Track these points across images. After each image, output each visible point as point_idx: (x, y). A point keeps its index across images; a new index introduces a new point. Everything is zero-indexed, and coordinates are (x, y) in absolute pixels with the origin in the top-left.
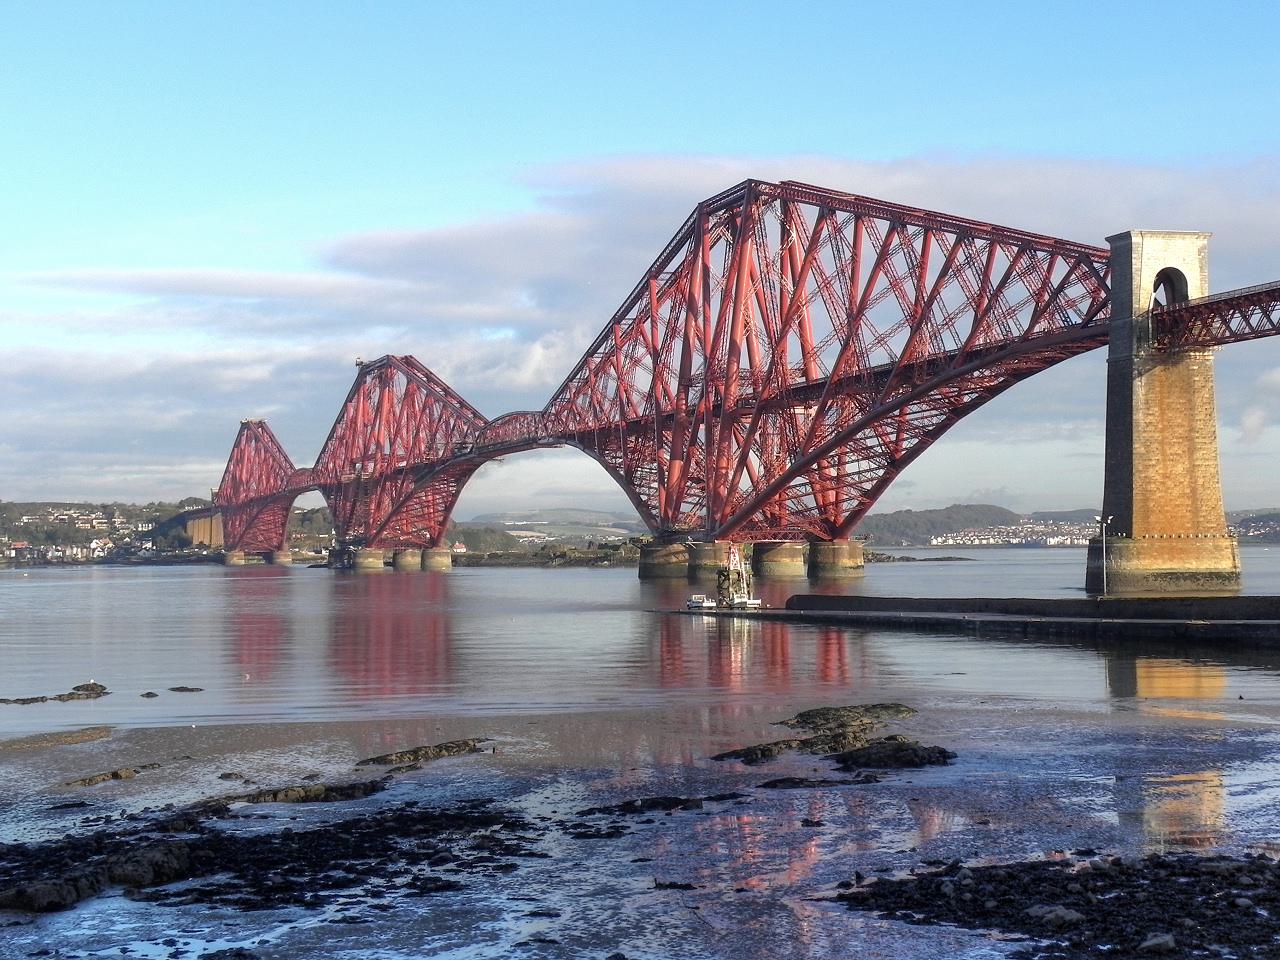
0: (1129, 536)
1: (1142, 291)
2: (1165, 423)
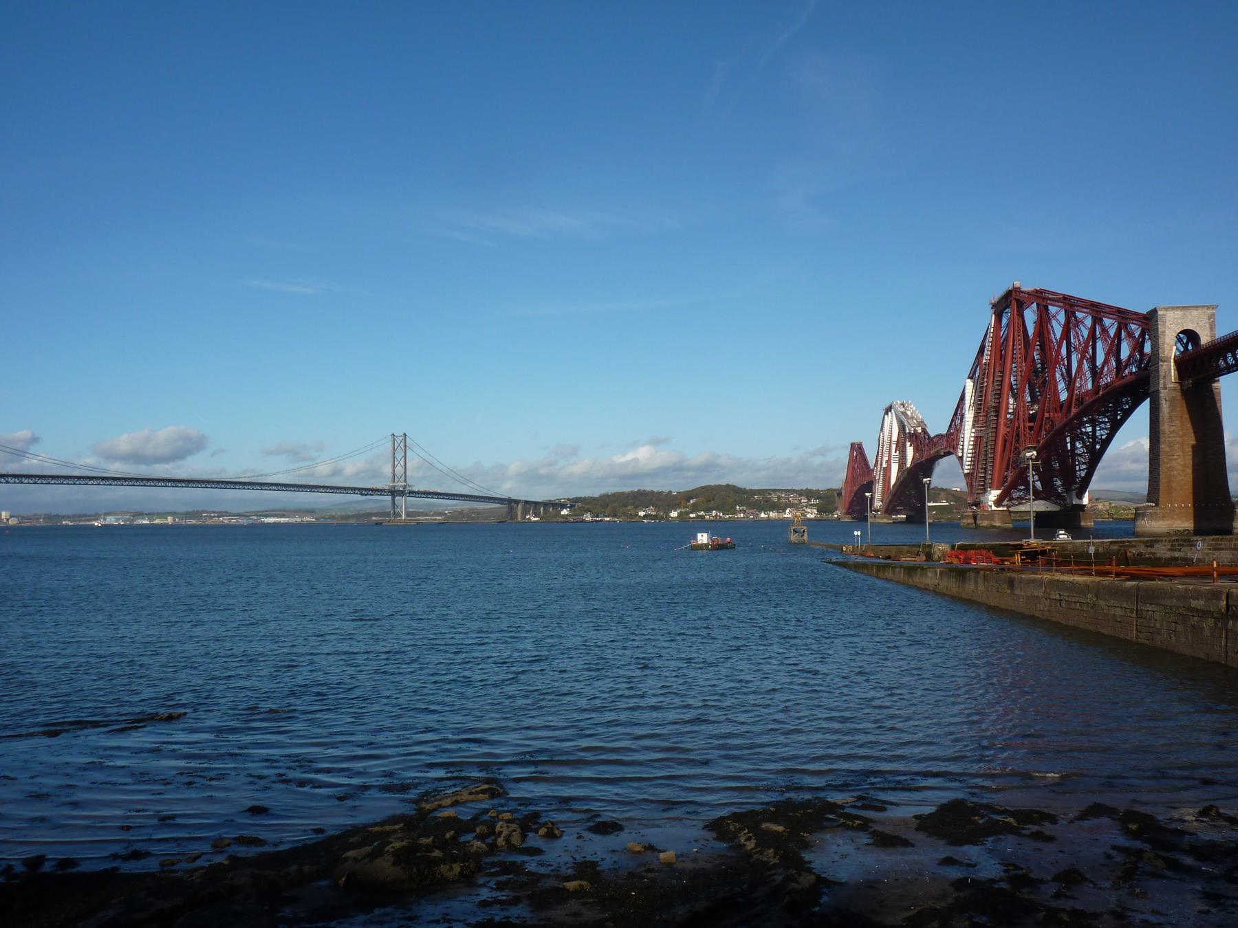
0: (1157, 505)
1: (1166, 346)
2: (1184, 431)
